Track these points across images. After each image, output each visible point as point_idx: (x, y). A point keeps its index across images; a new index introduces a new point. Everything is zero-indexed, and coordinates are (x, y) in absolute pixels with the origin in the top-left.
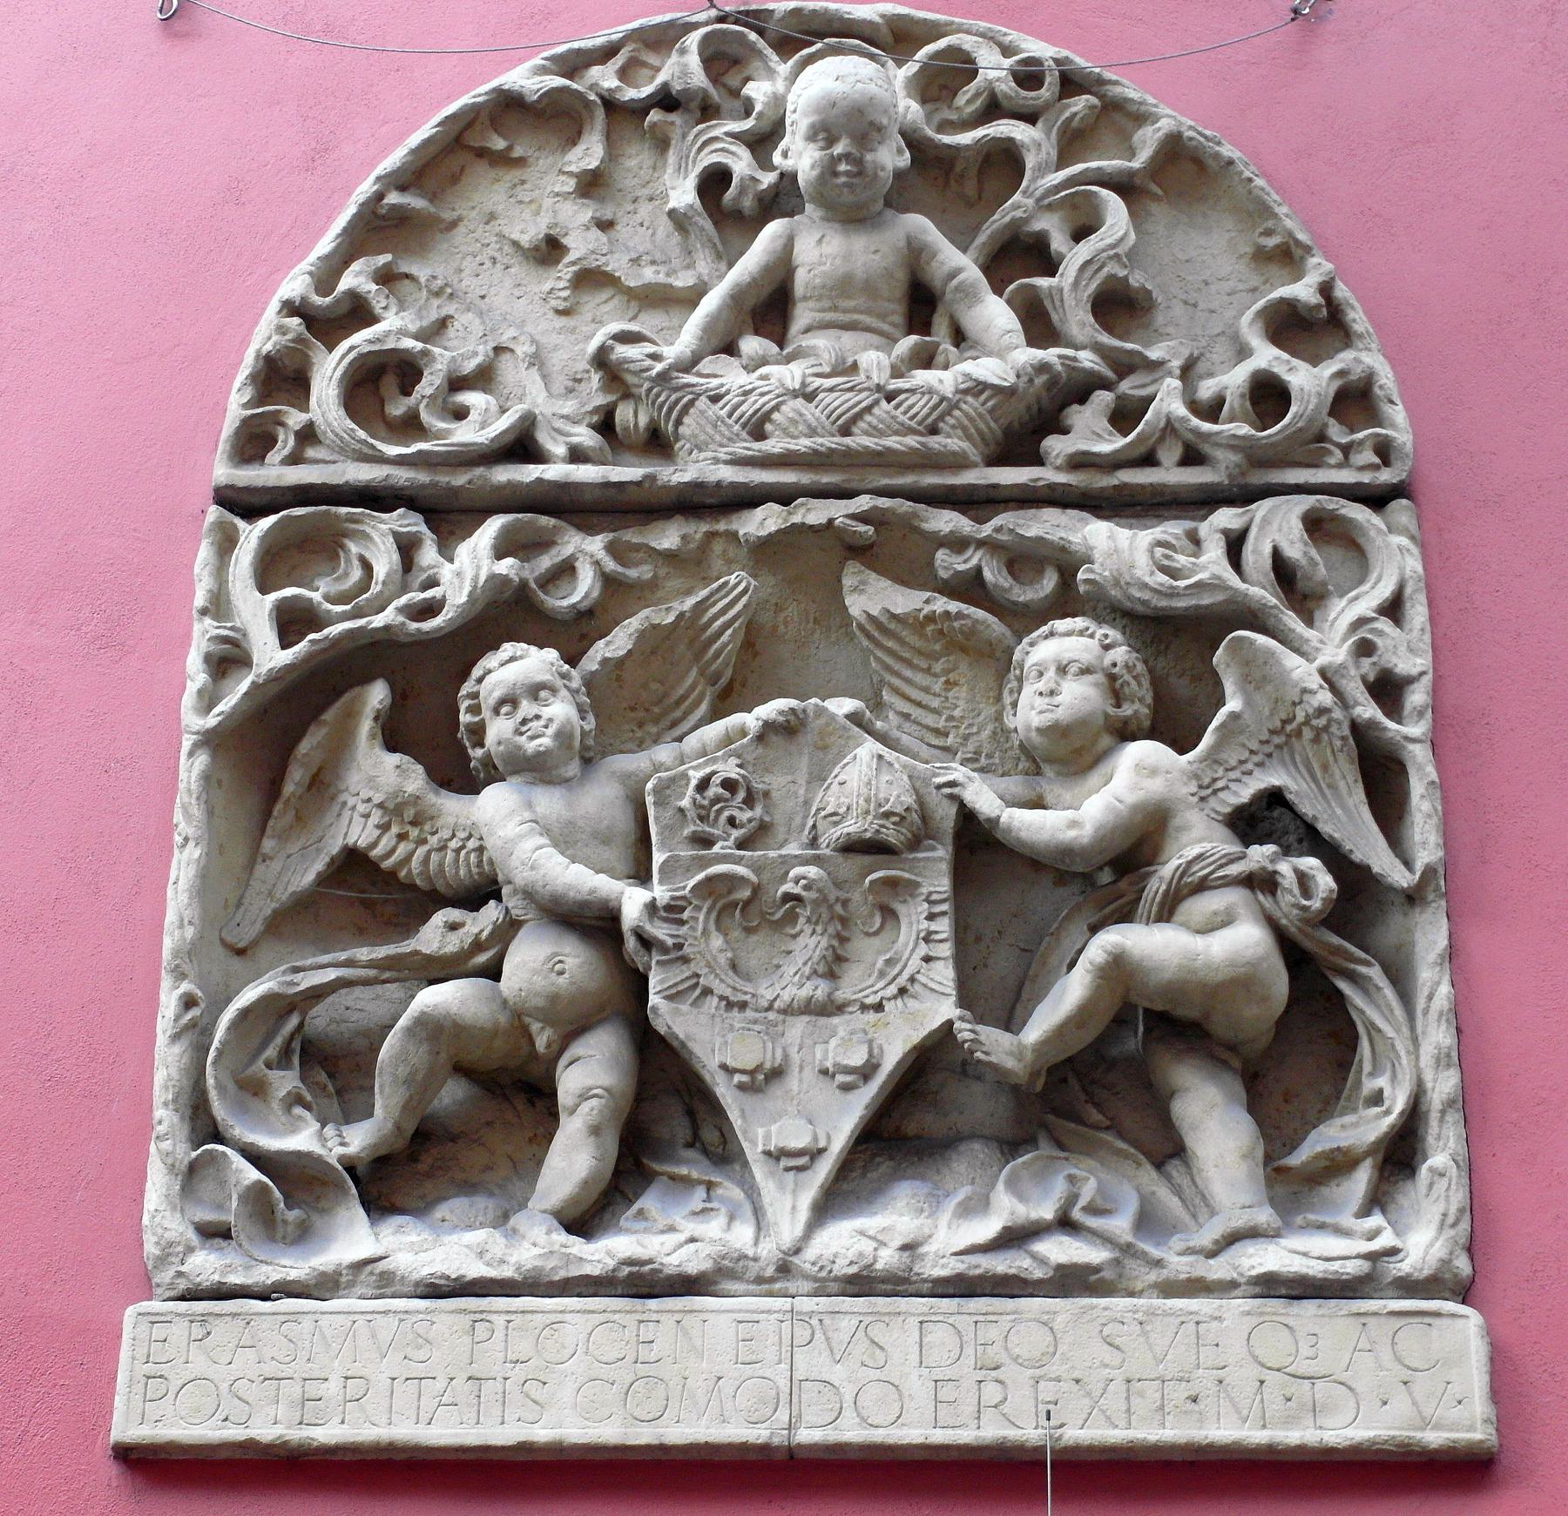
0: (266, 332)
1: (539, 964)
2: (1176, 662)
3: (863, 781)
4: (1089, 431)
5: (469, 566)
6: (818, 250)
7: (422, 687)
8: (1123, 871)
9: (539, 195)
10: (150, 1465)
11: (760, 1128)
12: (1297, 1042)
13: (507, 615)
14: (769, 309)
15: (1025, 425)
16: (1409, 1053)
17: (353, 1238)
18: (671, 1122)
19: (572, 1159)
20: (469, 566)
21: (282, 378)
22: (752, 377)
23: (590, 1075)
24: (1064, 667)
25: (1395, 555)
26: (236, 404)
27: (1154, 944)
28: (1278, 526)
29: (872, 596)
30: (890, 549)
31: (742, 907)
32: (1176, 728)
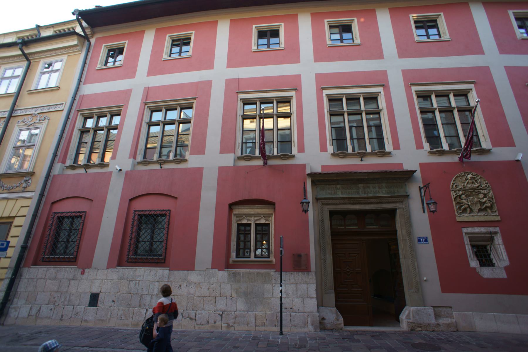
0: (451, 184)
1: (466, 206)
2: (485, 195)
3: (476, 200)
4: (480, 187)
5: (461, 192)
6: (470, 181)
7: (460, 196)
8: (485, 203)
9: (459, 179)
10: (458, 222)
11: (475, 211)
12: (491, 208)
13: (462, 194)
14: (468, 183)
15: (478, 187)
16: (495, 208)
17: (463, 215)
18: (471, 211)
19: (468, 212)
20: (461, 192)
21: (452, 186)
22: (468, 186)
23: (468, 209)
24: (481, 196)
25: (491, 191)
26: (451, 187)
27: (487, 205)
28: (488, 190)
29: (474, 193)
30: (474, 191)
31: (473, 204)
32: (486, 197)
